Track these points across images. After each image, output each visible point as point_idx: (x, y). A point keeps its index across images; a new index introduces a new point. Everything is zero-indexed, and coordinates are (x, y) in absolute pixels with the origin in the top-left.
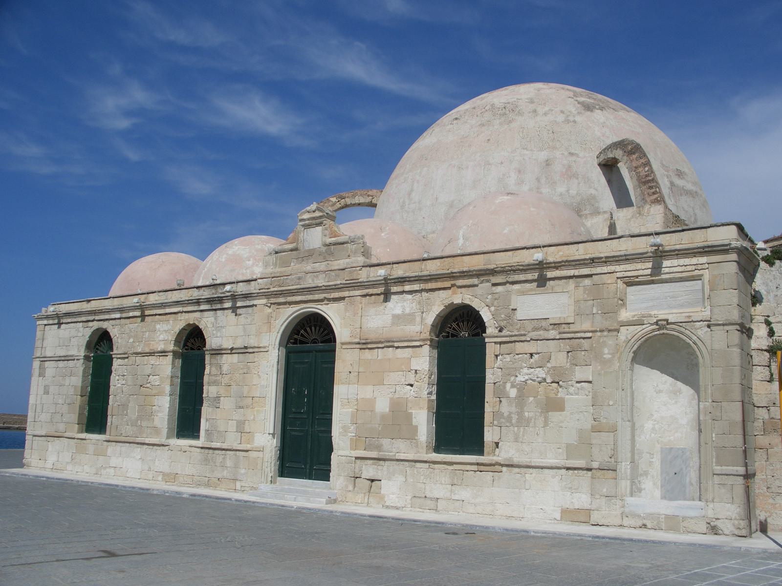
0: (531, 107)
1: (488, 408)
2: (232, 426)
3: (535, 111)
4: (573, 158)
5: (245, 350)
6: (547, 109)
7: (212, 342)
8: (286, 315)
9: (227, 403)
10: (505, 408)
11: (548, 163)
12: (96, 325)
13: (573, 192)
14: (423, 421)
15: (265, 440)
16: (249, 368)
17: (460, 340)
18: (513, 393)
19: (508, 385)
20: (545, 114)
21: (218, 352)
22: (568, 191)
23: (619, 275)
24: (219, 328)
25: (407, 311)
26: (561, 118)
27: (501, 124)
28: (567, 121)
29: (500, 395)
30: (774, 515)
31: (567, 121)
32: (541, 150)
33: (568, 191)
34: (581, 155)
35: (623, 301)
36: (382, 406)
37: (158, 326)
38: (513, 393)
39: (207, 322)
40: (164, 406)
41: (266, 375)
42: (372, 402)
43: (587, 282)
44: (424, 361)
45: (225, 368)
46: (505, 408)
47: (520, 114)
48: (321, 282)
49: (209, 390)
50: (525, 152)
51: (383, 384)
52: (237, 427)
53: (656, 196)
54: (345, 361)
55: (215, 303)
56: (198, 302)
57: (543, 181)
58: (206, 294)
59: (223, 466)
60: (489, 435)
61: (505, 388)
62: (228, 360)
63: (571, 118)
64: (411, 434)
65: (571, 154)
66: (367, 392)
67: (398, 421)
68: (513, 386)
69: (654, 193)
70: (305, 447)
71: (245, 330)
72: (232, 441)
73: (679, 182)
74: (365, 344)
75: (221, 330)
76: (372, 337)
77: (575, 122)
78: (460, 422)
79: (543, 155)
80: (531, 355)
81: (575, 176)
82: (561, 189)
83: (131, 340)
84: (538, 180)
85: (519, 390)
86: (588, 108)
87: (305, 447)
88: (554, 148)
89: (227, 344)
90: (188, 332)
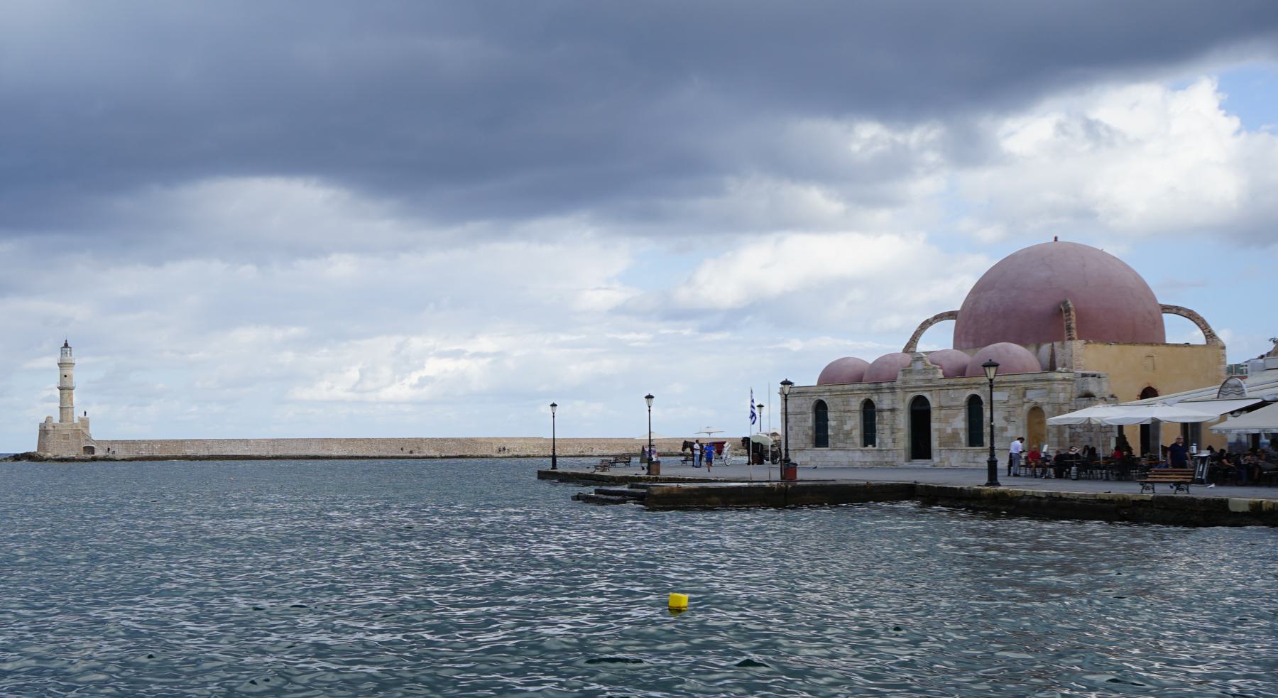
5: (893, 410)
7: (878, 406)
8: (911, 396)
12: (816, 398)
14: (963, 436)
21: (881, 410)
35: (1024, 395)
36: (949, 431)
39: (875, 398)
40: (857, 434)
41: (903, 421)
51: (949, 422)
54: (935, 415)
55: (878, 390)
62: (886, 414)
64: (960, 442)
67: (955, 434)
70: (920, 447)
72: (890, 446)
74: (941, 408)
75: (884, 402)
87: (920, 447)
89: (885, 407)
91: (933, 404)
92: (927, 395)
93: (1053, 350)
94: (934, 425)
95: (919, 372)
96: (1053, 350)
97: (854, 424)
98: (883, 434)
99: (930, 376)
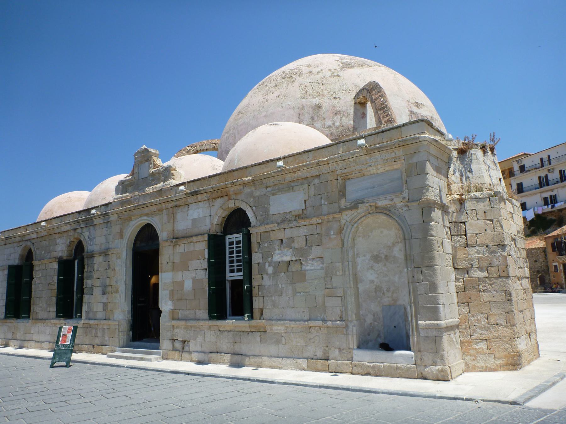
1: (255, 283)
2: (100, 307)
3: (311, 72)
4: (338, 100)
6: (319, 69)
7: (88, 248)
9: (97, 291)
10: (267, 282)
11: (319, 107)
13: (337, 124)
16: (109, 265)
18: (270, 270)
19: (267, 264)
20: (318, 73)
22: (333, 124)
23: (338, 173)
24: (92, 239)
25: (201, 216)
26: (329, 74)
27: (288, 84)
28: (333, 76)
30: (478, 358)
31: (333, 76)
32: (314, 98)
33: (333, 124)
34: (342, 98)
37: (58, 241)
38: (270, 270)
39: (85, 235)
42: (182, 284)
43: (316, 181)
45: (96, 267)
47: (301, 74)
50: (303, 100)
52: (103, 307)
53: (388, 118)
54: (167, 255)
56: (78, 222)
57: (316, 118)
59: (96, 336)
60: (257, 303)
61: (265, 266)
62: (98, 260)
63: (336, 74)
65: (335, 98)
66: (180, 276)
68: (270, 265)
69: (387, 116)
71: (106, 239)
73: (415, 110)
76: (180, 235)
77: (338, 76)
79: (316, 101)
80: (282, 240)
81: (337, 113)
82: (329, 123)
83: (43, 252)
84: (312, 118)
85: (274, 267)
86: (350, 66)
88: (324, 95)
90: (76, 243)
91: (163, 235)
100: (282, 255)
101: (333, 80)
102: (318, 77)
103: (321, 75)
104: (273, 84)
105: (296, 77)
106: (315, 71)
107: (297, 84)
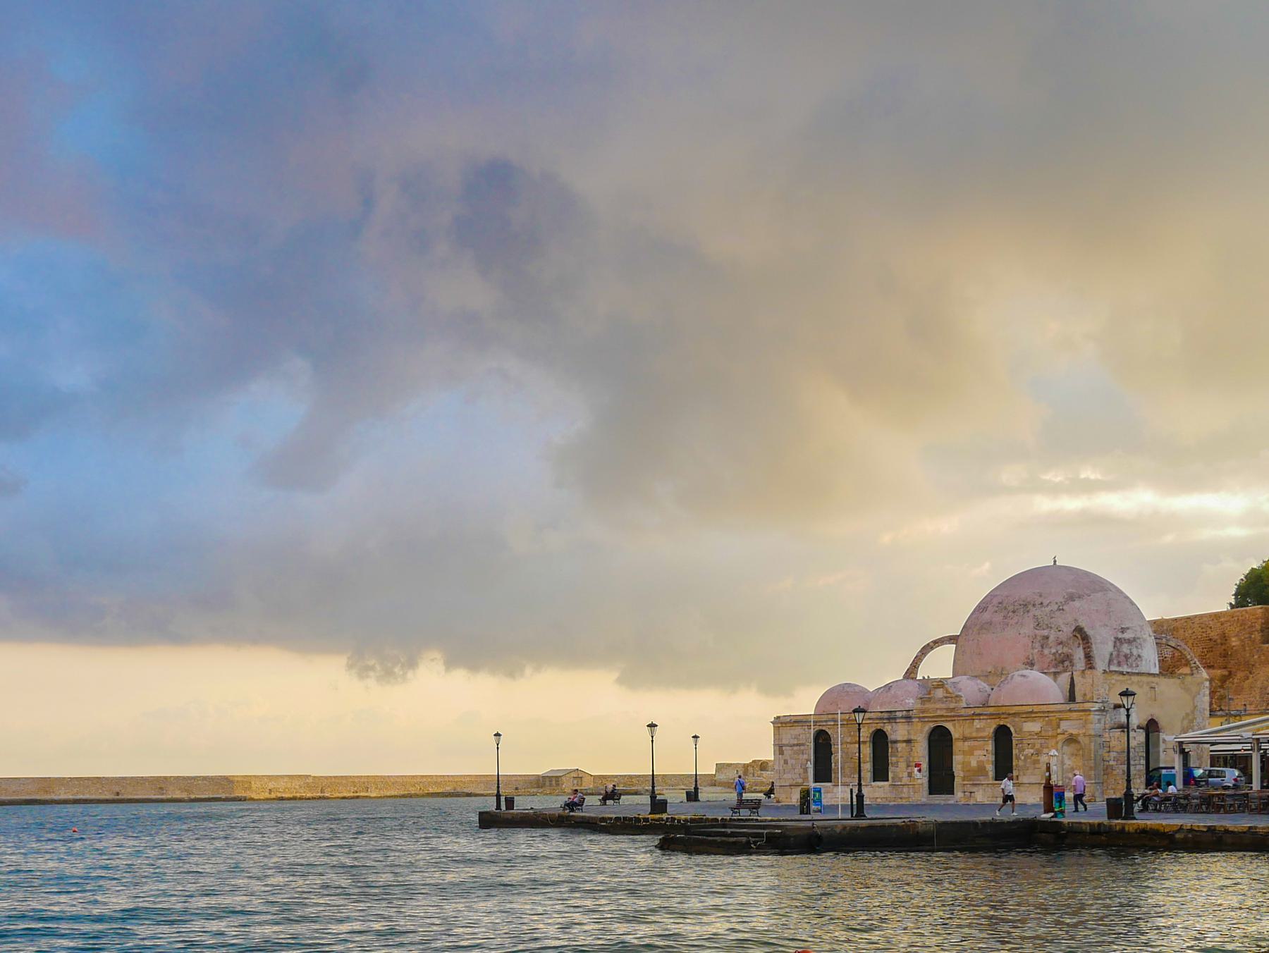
0: (1040, 600)
2: (905, 774)
5: (909, 741)
7: (891, 737)
14: (990, 768)
15: (922, 778)
17: (1003, 737)
21: (896, 742)
26: (1056, 607)
29: (1018, 758)
35: (1059, 726)
36: (974, 764)
39: (888, 728)
41: (921, 751)
44: (990, 746)
46: (1021, 763)
48: (943, 713)
49: (892, 759)
51: (973, 755)
54: (958, 746)
58: (886, 715)
62: (900, 746)
64: (986, 775)
67: (981, 770)
70: (941, 780)
72: (905, 780)
73: (1120, 635)
74: (965, 739)
75: (897, 732)
78: (1004, 767)
79: (1045, 633)
87: (941, 780)
89: (899, 738)
91: (955, 735)
92: (949, 726)
93: (1072, 679)
94: (957, 759)
95: (940, 700)
96: (1072, 679)
97: (984, 755)
98: (898, 769)
99: (952, 705)
100: (1029, 751)
101: (1058, 613)
102: (1048, 609)
103: (1049, 608)
104: (1011, 608)
105: (1030, 607)
106: (1046, 602)
107: (1031, 614)
